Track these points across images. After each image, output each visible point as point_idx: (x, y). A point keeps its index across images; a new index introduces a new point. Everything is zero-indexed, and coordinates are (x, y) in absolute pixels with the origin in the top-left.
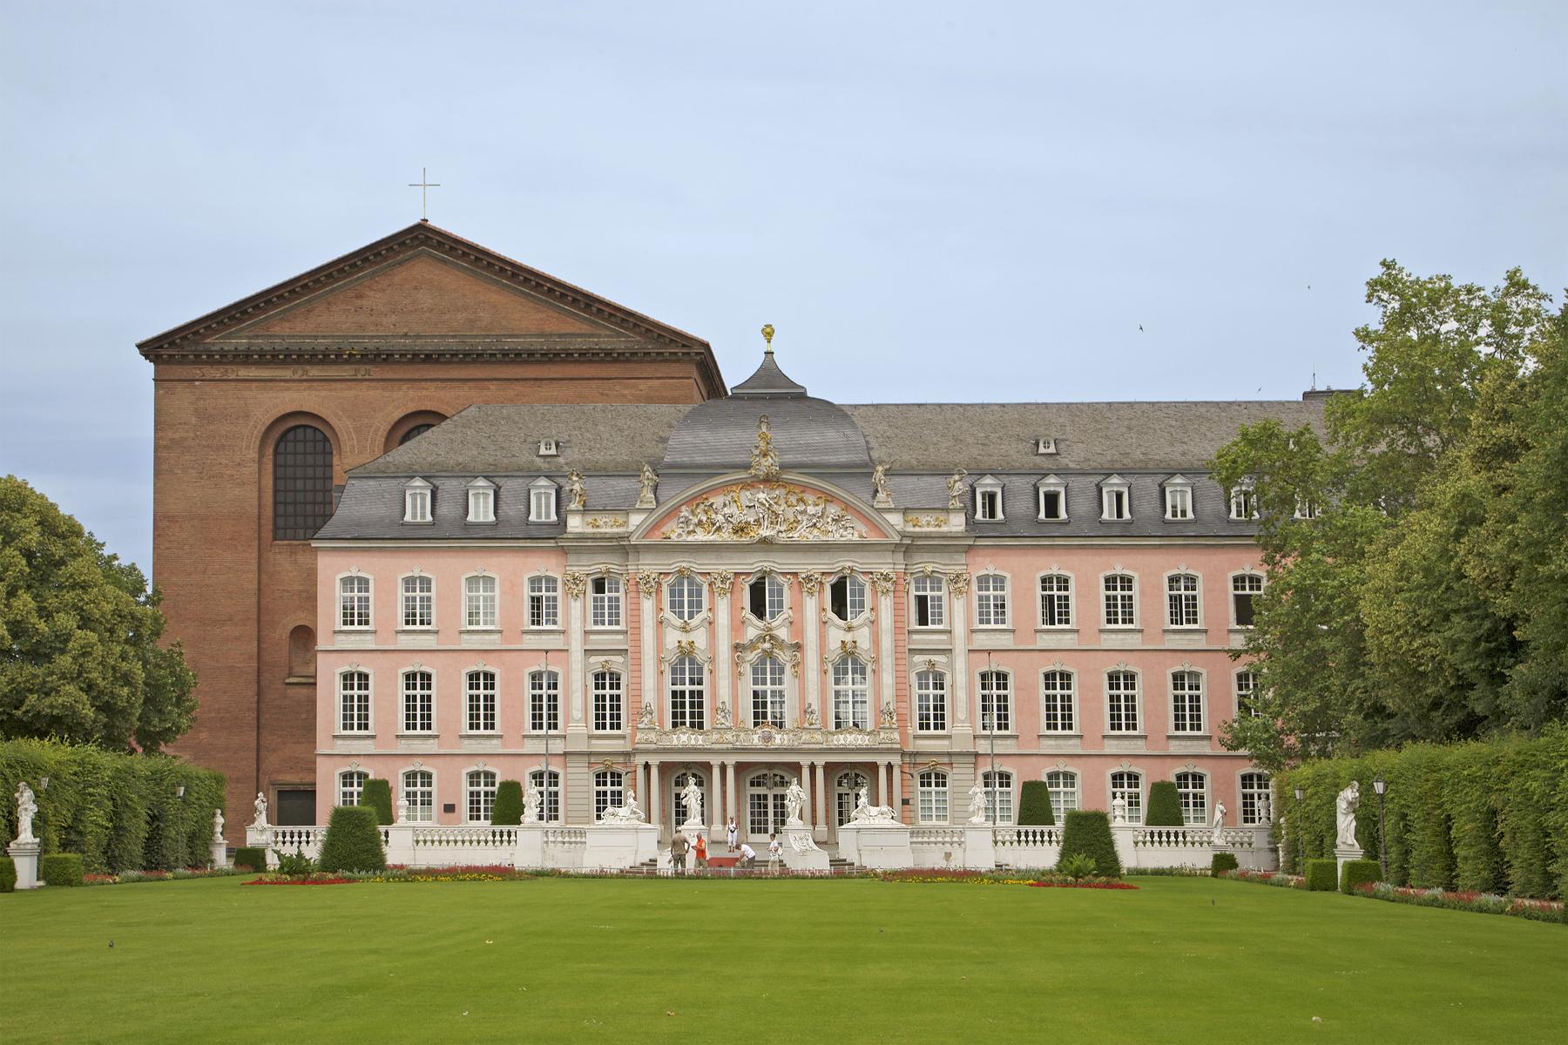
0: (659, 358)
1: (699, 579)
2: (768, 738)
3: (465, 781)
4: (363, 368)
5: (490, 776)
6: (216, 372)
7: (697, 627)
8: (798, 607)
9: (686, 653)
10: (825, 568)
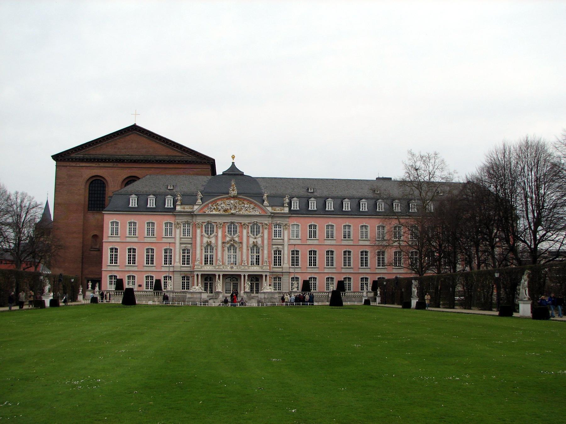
0: (201, 163)
1: (213, 224)
3: (145, 278)
6: (74, 164)
8: (242, 232)
10: (249, 222)
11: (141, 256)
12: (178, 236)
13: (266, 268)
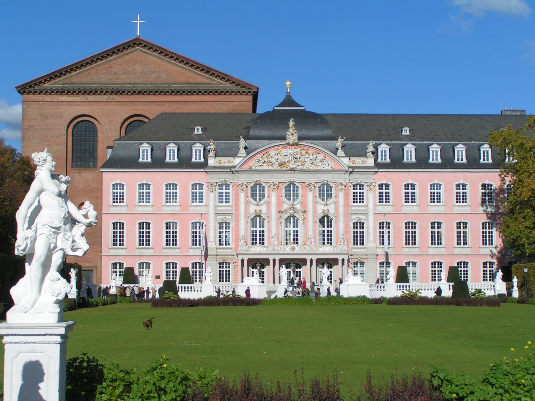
2: (293, 249)
3: (164, 266)
4: (111, 97)
5: (121, 264)
7: (263, 204)
8: (305, 196)
9: (258, 215)
10: (316, 180)
11: (158, 234)
12: (212, 204)
13: (343, 248)
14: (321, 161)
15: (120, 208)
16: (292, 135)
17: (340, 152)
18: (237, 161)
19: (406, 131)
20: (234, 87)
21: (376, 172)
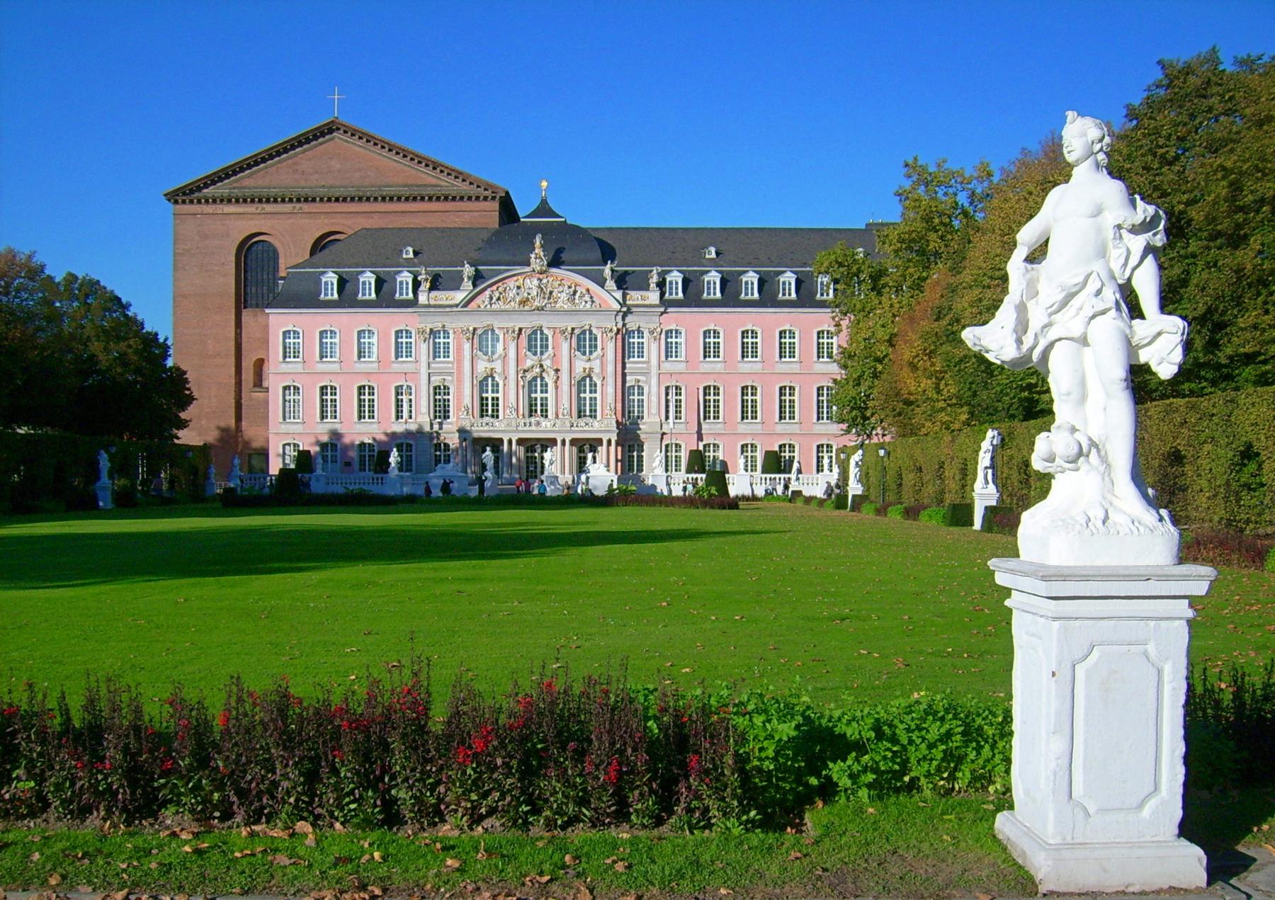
2: (538, 424)
6: (209, 209)
12: (424, 359)
14: (587, 298)
15: (294, 365)
16: (538, 257)
17: (611, 284)
18: (459, 296)
19: (710, 253)
20: (473, 191)
21: (662, 313)
